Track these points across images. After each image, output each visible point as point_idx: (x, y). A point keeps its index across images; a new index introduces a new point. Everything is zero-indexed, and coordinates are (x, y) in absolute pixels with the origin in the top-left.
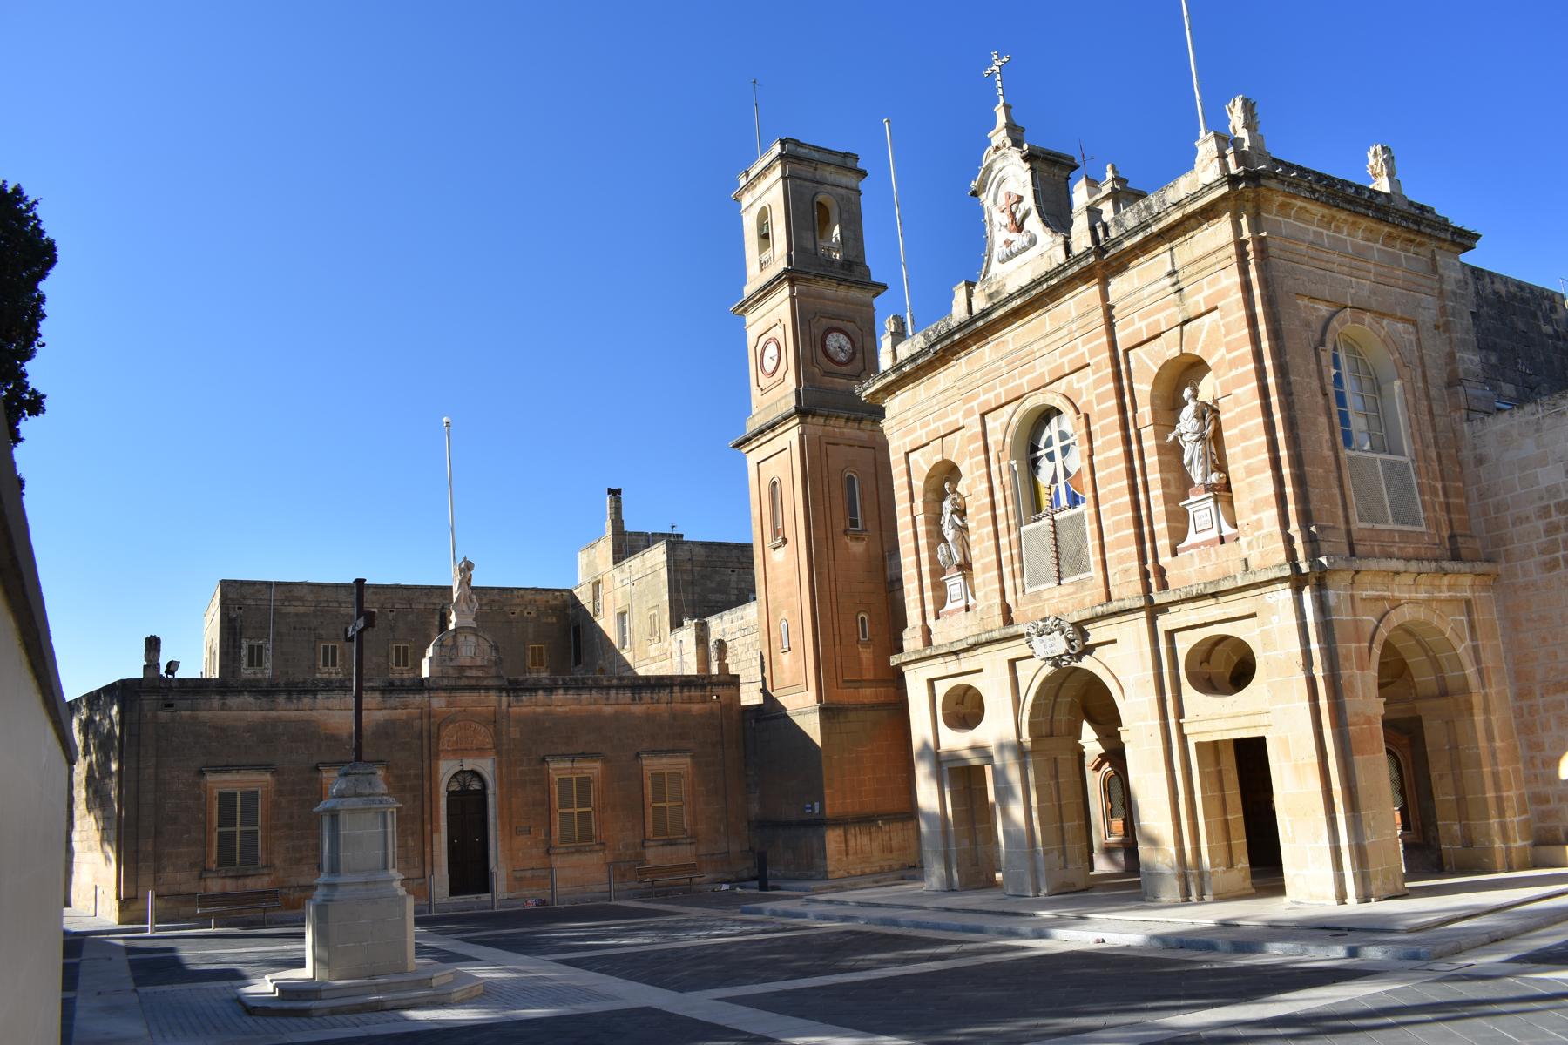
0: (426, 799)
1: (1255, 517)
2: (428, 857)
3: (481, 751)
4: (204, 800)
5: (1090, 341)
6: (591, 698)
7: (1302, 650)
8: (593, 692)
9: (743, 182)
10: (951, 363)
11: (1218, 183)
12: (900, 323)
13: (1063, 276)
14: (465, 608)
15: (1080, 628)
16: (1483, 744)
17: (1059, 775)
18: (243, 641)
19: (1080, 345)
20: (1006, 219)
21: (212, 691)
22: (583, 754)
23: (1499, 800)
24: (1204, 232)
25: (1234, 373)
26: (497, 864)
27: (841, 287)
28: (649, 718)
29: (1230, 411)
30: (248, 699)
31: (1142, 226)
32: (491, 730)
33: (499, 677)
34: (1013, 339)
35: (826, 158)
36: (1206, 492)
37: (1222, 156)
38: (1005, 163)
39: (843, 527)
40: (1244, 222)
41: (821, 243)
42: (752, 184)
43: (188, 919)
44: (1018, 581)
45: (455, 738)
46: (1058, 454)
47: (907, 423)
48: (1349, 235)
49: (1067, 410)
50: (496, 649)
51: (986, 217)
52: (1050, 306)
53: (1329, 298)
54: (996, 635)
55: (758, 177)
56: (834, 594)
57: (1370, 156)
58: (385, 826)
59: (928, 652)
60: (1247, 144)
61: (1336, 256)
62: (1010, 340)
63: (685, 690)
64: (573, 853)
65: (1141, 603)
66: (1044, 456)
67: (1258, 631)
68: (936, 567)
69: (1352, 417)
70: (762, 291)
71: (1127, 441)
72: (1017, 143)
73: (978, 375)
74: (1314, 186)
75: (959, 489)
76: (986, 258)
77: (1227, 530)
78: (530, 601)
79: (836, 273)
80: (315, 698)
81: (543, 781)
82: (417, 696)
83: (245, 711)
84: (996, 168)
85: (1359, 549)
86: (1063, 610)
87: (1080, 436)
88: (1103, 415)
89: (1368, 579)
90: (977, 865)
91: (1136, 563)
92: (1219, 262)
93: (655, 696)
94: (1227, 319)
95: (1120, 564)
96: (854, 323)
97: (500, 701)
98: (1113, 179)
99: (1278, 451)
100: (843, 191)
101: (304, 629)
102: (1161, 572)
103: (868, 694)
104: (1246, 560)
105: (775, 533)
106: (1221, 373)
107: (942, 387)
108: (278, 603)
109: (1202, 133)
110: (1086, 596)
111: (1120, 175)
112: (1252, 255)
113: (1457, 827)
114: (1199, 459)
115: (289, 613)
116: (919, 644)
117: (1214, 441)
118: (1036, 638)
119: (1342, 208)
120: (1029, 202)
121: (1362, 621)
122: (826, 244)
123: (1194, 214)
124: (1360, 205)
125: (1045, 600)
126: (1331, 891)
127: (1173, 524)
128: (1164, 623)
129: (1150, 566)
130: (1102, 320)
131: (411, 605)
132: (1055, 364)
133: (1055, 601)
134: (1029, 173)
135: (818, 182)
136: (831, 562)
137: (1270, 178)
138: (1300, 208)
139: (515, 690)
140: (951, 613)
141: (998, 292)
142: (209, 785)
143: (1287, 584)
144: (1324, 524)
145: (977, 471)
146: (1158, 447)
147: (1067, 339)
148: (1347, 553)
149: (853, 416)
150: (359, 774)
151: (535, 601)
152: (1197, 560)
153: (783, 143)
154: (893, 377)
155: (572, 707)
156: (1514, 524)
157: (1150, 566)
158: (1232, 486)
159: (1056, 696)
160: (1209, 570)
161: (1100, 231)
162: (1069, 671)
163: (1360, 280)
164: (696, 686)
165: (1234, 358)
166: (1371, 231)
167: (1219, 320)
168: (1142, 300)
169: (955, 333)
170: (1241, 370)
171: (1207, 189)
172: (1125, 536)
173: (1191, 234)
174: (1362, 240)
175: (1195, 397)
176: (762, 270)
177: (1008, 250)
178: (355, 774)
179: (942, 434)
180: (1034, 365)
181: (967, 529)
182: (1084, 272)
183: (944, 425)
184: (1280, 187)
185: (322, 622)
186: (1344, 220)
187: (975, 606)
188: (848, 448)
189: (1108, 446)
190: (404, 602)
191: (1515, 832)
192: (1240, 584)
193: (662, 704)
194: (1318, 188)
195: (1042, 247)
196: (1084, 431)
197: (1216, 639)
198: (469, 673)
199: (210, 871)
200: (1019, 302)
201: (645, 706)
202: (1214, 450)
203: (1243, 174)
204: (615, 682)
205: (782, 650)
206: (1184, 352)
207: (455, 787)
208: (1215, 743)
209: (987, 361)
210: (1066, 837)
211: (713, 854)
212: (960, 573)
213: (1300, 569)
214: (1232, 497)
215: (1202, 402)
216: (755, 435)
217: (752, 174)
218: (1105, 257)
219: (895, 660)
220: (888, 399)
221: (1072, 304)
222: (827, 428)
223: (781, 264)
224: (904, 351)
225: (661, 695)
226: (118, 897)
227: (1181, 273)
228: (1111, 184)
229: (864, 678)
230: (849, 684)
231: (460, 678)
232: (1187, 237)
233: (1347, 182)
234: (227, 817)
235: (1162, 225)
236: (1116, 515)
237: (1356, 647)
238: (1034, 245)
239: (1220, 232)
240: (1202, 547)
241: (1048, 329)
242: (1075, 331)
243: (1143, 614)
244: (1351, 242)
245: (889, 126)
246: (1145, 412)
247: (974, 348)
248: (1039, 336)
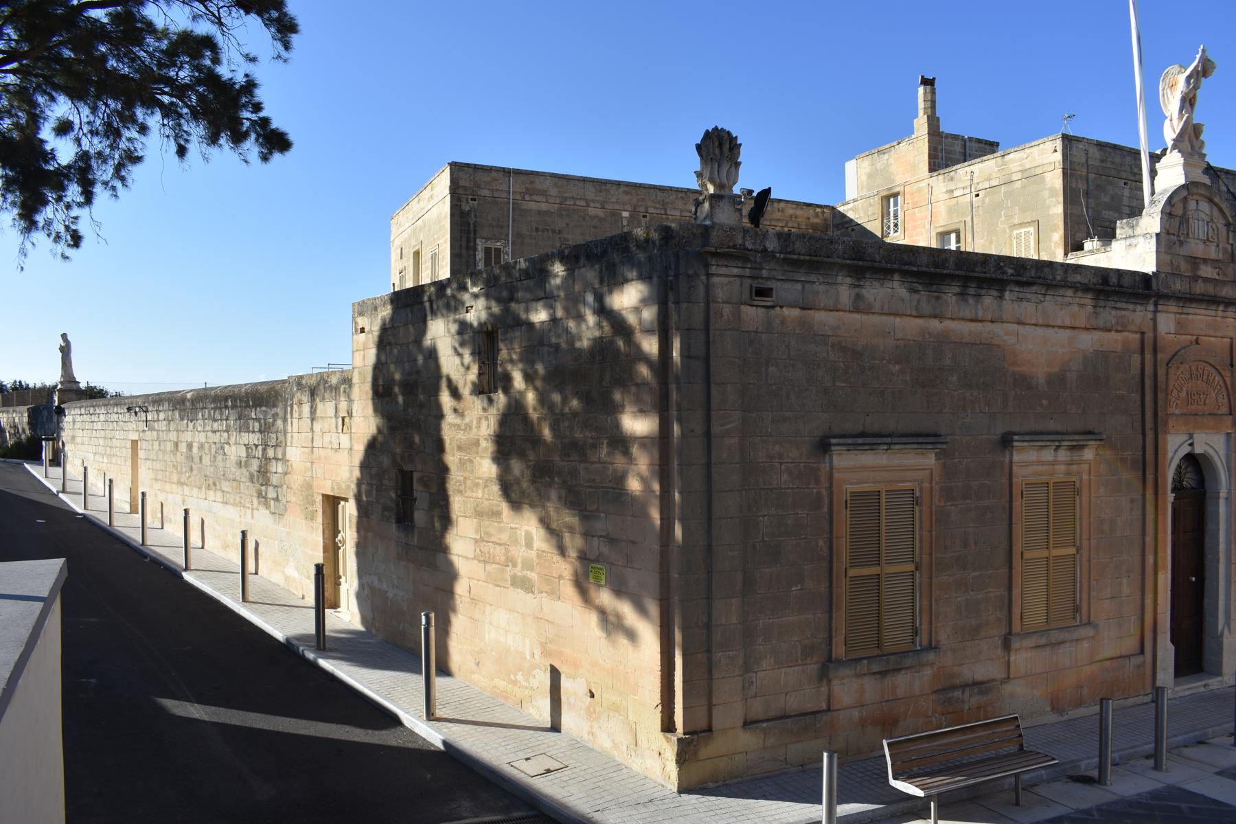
4: (826, 509)
18: (478, 241)
21: (842, 266)
30: (896, 289)
78: (791, 216)
80: (1001, 297)
82: (1139, 308)
108: (518, 197)
115: (531, 210)
131: (666, 210)
151: (796, 217)
185: (567, 224)
190: (657, 206)
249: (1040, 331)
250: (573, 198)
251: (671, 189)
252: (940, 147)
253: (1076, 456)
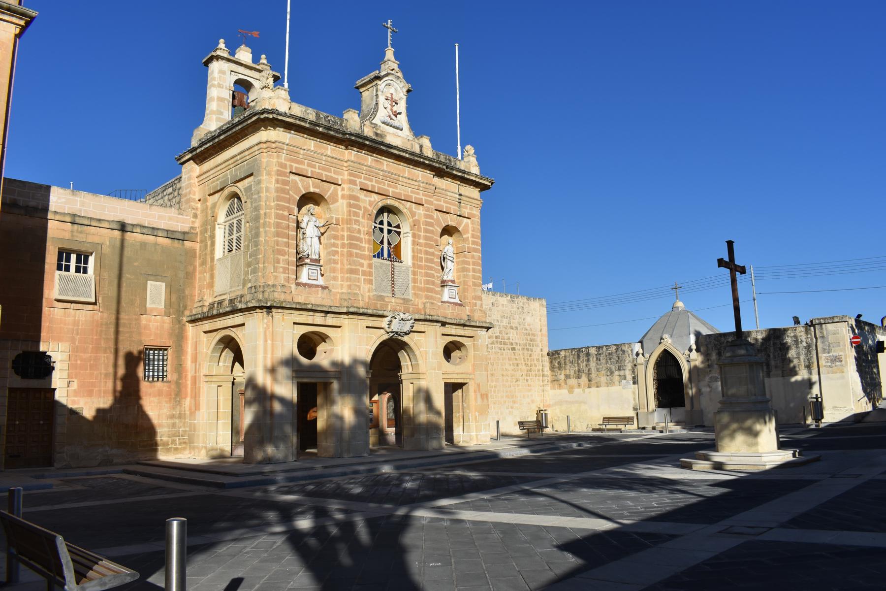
10: (340, 146)
13: (431, 163)
46: (385, 231)
52: (411, 167)
73: (365, 168)
107: (329, 153)
160: (455, 314)
170: (476, 247)
192: (477, 325)
200: (407, 156)
220: (282, 129)
247: (364, 152)
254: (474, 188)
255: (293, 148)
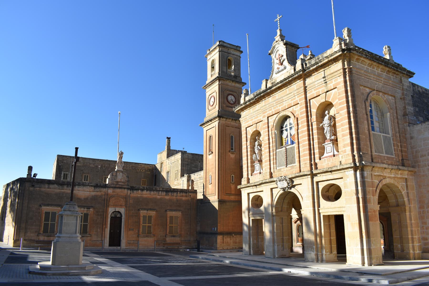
0: (104, 218)
1: (344, 149)
2: (103, 235)
3: (121, 206)
4: (41, 214)
5: (299, 96)
6: (154, 193)
7: (356, 189)
8: (155, 192)
9: (208, 52)
11: (338, 51)
12: (247, 91)
13: (293, 77)
14: (120, 165)
15: (291, 180)
16: (408, 221)
17: (283, 223)
18: (62, 172)
19: (297, 97)
20: (278, 61)
21: (46, 183)
22: (150, 209)
23: (413, 238)
24: (334, 66)
25: (340, 106)
26: (123, 239)
27: (233, 83)
28: (170, 200)
29: (339, 118)
30: (56, 186)
31: (316, 63)
32: (125, 200)
33: (128, 185)
34: (278, 96)
35: (231, 47)
36: (330, 141)
37: (340, 44)
38: (279, 46)
39: (229, 150)
40: (346, 63)
41: (228, 70)
42: (211, 53)
43: (33, 247)
44: (275, 165)
45: (114, 202)
47: (247, 119)
48: (376, 70)
49: (292, 116)
50: (128, 177)
51: (273, 61)
52: (289, 86)
53: (369, 87)
54: (267, 181)
55: (212, 51)
56: (225, 169)
57: (384, 49)
58: (77, 221)
59: (248, 185)
60: (348, 41)
61: (372, 75)
62: (277, 96)
63: (181, 193)
64: (145, 237)
65: (309, 173)
66: (285, 130)
67: (343, 183)
68: (252, 161)
69: (375, 122)
70: (211, 82)
71: (308, 126)
72: (282, 40)
73: (267, 106)
74: (367, 54)
75: (260, 139)
76: (272, 72)
77: (336, 153)
78: (143, 167)
79: (232, 79)
81: (138, 216)
82: (104, 189)
83: (55, 189)
84: (276, 47)
85: (374, 160)
86: (287, 174)
87: (295, 124)
88: (302, 118)
89: (377, 169)
90: (258, 248)
91: (309, 161)
92: (338, 74)
93: (172, 194)
94: (339, 91)
95: (304, 161)
96: (236, 93)
97: (128, 192)
98: (311, 55)
99: (352, 130)
100: (236, 56)
101: (80, 170)
102: (316, 164)
103: (232, 198)
104: (341, 162)
105: (210, 150)
106: (337, 107)
107: (257, 109)
109: (335, 38)
110: (294, 170)
111: (313, 54)
112: (347, 73)
113: (399, 246)
114: (329, 132)
116: (246, 183)
117: (334, 127)
118: (278, 182)
119: (375, 61)
120: (285, 57)
121: (374, 181)
122: (230, 71)
123: (331, 60)
124: (380, 61)
125: (282, 171)
126: (360, 262)
127: (320, 151)
128: (316, 179)
129: (313, 162)
130: (303, 91)
132: (289, 103)
133: (285, 171)
134: (285, 48)
135: (229, 53)
136: (225, 159)
137: (354, 50)
138: (363, 60)
139: (132, 189)
140: (255, 174)
141: (274, 82)
142: (42, 209)
143: (352, 169)
144: (365, 152)
145: (265, 133)
146: (317, 128)
147: (293, 96)
148: (371, 160)
149: (234, 119)
150: (71, 204)
151: (145, 167)
152: (326, 161)
153: (220, 42)
154: (243, 106)
155: (149, 195)
156: (421, 157)
157: (313, 162)
158: (338, 140)
159: (284, 200)
160: (330, 164)
161: (304, 65)
162: (288, 193)
163: (379, 83)
164: (184, 192)
165: (341, 102)
166: (383, 69)
167: (337, 91)
168: (315, 85)
169: (261, 93)
170: (342, 106)
171: (335, 53)
172: (306, 153)
173: (330, 66)
174: (380, 71)
175: (329, 114)
176: (211, 77)
177: (278, 70)
178: (70, 204)
179: (256, 123)
180: (283, 103)
181: (261, 150)
182: (299, 77)
183: (257, 120)
184: (357, 53)
185: (85, 169)
186: (375, 65)
187: (262, 172)
188: (232, 128)
189: (303, 127)
190: (108, 165)
191: (417, 248)
192: (338, 169)
193: (174, 197)
194: (368, 55)
195: (288, 69)
196: (296, 122)
197: (332, 184)
198: (120, 183)
199: (41, 234)
200: (280, 85)
201: (169, 197)
202: (333, 129)
203: (346, 49)
204: (161, 189)
205: (209, 184)
206: (326, 100)
207: (113, 216)
208: (329, 215)
209: (270, 101)
210: (284, 241)
211: (186, 240)
212: (259, 163)
213: (356, 165)
214: (338, 143)
215: (330, 115)
216: (206, 123)
217: (211, 50)
218: (305, 72)
219: (239, 187)
221: (295, 86)
222: (226, 122)
223: (217, 75)
224: (247, 98)
225: (174, 194)
226: (14, 239)
227: (327, 77)
228: (310, 56)
229: (232, 193)
230: (228, 195)
231: (117, 185)
232: (329, 67)
233: (377, 55)
234: (47, 219)
235: (322, 63)
236: (304, 147)
237: (372, 189)
238: (286, 69)
239: (339, 65)
240: (328, 158)
241: (288, 93)
242: (296, 94)
243: (310, 176)
244: (377, 72)
245: (248, 36)
246: (314, 118)
247: (267, 98)
248: (285, 95)
249: (83, 192)
250: (86, 163)
251: (112, 161)
252: (170, 153)
253: (88, 210)
254: (338, 62)
255: (245, 117)
